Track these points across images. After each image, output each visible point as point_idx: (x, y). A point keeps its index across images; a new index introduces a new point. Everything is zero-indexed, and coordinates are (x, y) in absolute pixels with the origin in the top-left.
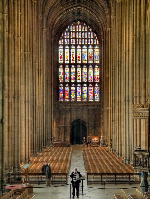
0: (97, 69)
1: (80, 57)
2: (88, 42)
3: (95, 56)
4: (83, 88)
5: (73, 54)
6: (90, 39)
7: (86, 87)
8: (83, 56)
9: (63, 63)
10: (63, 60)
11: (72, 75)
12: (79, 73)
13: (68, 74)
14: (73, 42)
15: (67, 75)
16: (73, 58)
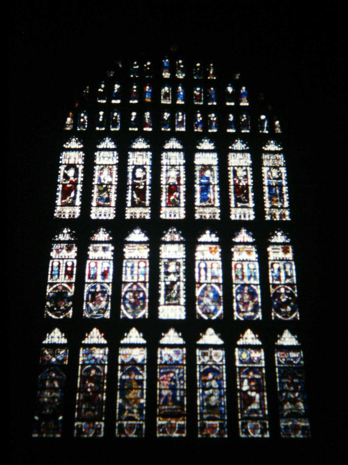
0: (286, 251)
1: (183, 189)
2: (223, 124)
3: (266, 189)
4: (198, 352)
5: (139, 173)
6: (238, 111)
7: (216, 347)
8: (198, 188)
9: (77, 215)
10: (78, 202)
11: (127, 277)
12: (172, 268)
13: (105, 274)
14: (140, 122)
15: (99, 279)
16: (141, 193)
